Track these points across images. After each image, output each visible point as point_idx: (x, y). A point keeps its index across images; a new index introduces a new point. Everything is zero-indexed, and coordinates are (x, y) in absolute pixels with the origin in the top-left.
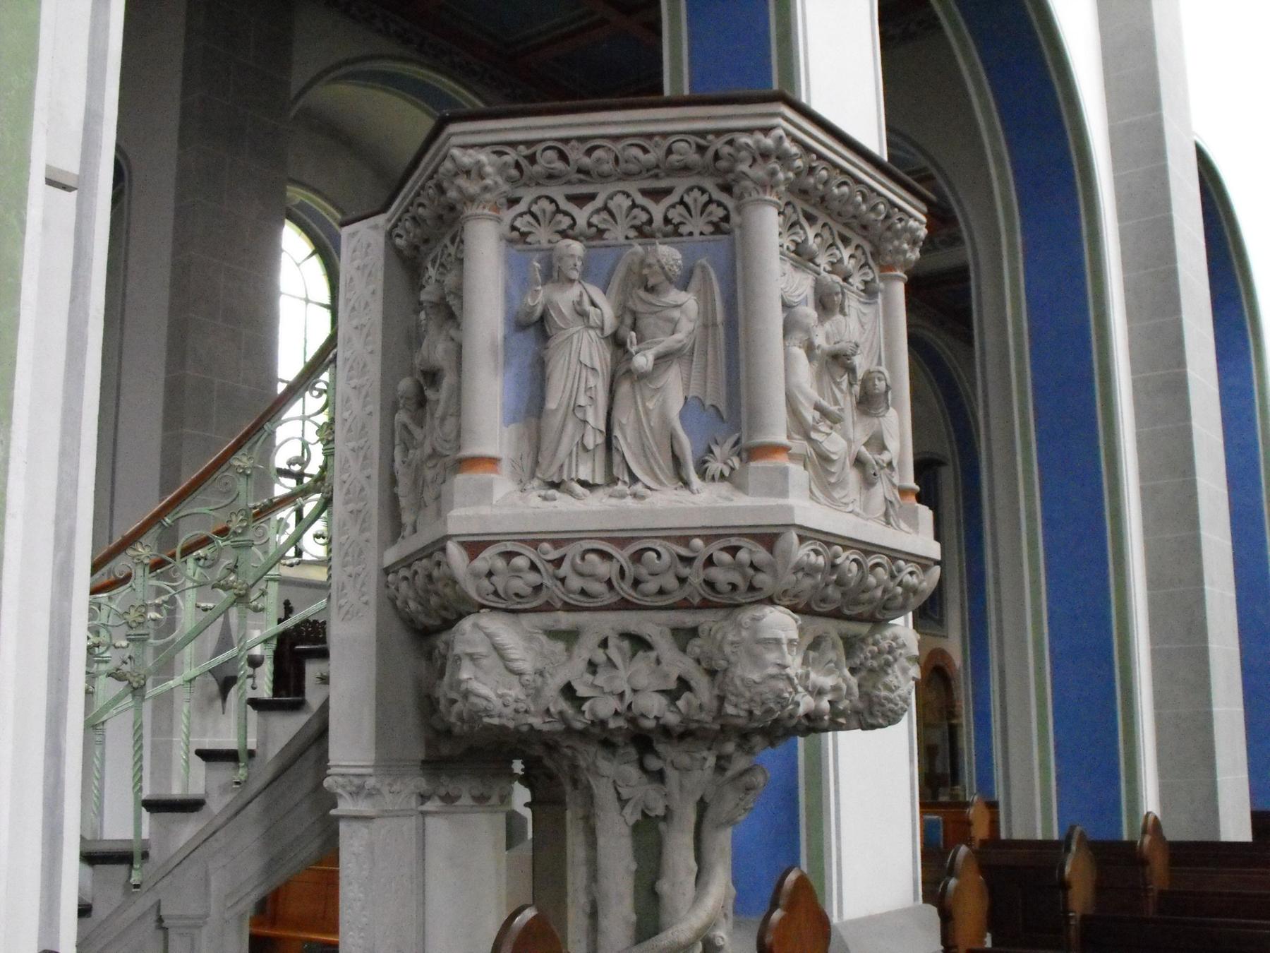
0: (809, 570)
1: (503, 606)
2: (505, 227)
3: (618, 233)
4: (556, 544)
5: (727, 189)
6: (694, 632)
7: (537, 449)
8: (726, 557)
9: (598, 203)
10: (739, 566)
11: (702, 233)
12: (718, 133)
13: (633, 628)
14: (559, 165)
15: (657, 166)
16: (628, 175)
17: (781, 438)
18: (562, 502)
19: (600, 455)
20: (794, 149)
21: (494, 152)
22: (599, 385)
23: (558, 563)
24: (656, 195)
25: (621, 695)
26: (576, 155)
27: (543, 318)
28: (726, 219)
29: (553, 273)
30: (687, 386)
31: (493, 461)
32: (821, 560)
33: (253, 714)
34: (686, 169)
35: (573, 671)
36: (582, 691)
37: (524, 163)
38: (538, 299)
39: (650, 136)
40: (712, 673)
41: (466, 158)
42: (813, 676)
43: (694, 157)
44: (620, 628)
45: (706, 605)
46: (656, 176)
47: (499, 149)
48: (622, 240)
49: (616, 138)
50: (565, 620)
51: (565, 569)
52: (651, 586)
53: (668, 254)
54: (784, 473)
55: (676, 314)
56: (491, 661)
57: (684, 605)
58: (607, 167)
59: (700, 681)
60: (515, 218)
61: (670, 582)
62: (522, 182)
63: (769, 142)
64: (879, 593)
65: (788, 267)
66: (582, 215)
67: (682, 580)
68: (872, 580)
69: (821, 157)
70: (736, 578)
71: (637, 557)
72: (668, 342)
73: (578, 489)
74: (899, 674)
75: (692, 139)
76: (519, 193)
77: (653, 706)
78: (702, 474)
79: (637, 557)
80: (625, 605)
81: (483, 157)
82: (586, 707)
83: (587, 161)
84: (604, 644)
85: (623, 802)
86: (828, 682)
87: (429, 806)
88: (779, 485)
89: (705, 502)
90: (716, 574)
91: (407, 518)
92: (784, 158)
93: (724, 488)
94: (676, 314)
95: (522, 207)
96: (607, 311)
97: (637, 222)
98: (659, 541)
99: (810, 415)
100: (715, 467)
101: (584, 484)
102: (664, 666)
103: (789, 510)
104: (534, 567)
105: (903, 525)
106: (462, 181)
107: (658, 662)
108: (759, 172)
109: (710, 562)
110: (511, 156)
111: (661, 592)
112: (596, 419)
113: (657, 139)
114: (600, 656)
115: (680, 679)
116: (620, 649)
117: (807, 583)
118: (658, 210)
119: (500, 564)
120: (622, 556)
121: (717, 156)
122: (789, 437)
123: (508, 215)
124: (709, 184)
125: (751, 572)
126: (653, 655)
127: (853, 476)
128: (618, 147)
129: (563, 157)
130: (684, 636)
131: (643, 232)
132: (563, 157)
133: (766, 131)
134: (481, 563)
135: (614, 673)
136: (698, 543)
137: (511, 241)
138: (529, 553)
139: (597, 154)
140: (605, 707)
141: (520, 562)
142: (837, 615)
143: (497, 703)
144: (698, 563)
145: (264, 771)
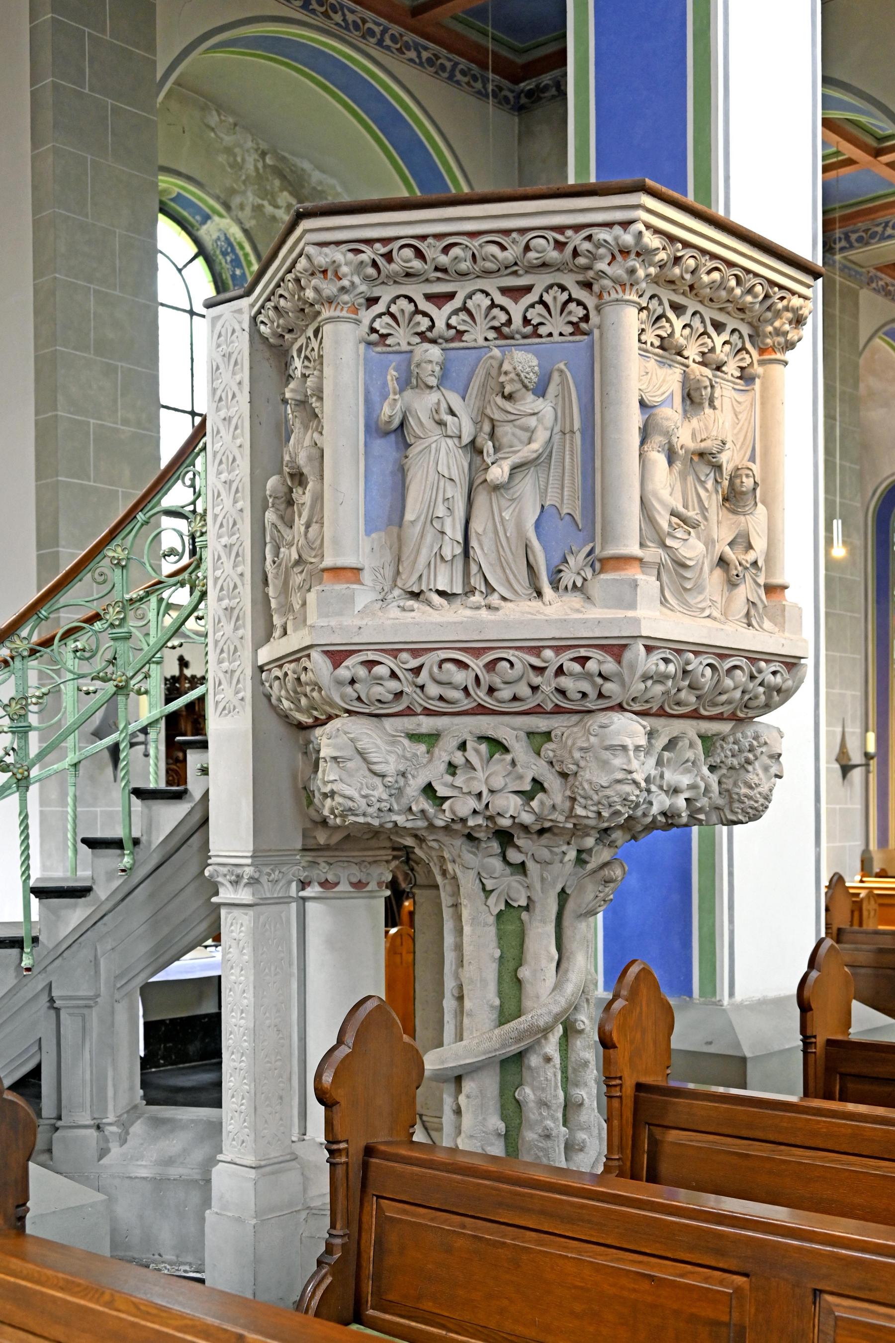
0: (661, 678)
1: (367, 711)
3: (478, 334)
4: (416, 653)
5: (587, 285)
6: (547, 736)
8: (577, 667)
9: (457, 303)
10: (588, 676)
11: (561, 334)
12: (577, 228)
13: (490, 733)
14: (417, 264)
15: (516, 264)
16: (487, 273)
17: (634, 549)
18: (420, 613)
19: (459, 564)
23: (417, 671)
25: (479, 795)
26: (432, 250)
29: (409, 380)
30: (544, 493)
35: (433, 772)
36: (442, 792)
37: (381, 261)
39: (507, 232)
40: (564, 775)
42: (668, 775)
43: (553, 255)
44: (479, 733)
45: (558, 711)
46: (515, 273)
47: (355, 246)
48: (481, 342)
49: (473, 235)
50: (426, 724)
52: (506, 693)
53: (524, 360)
54: (635, 585)
55: (532, 422)
57: (537, 711)
58: (463, 266)
59: (552, 781)
60: (374, 320)
61: (524, 690)
63: (628, 238)
64: (737, 694)
65: (652, 364)
67: (535, 689)
68: (728, 682)
69: (686, 245)
70: (586, 686)
73: (436, 599)
74: (760, 772)
77: (510, 806)
78: (555, 585)
79: (491, 666)
80: (481, 710)
81: (338, 255)
82: (446, 806)
83: (443, 260)
84: (463, 746)
85: (487, 893)
86: (685, 780)
88: (628, 597)
89: (556, 614)
90: (565, 682)
91: (277, 620)
92: (644, 253)
93: (575, 600)
94: (532, 422)
95: (380, 308)
97: (496, 324)
98: (511, 652)
99: (663, 521)
100: (568, 578)
101: (442, 594)
102: (519, 769)
103: (637, 621)
104: (393, 675)
105: (767, 624)
107: (513, 763)
108: (618, 270)
109: (560, 671)
110: (368, 254)
111: (515, 698)
113: (514, 235)
114: (458, 758)
115: (534, 780)
116: (477, 751)
117: (659, 689)
118: (517, 310)
119: (362, 672)
120: (477, 665)
121: (575, 253)
122: (642, 545)
123: (366, 316)
125: (599, 681)
126: (508, 757)
129: (419, 254)
130: (538, 739)
132: (419, 254)
133: (626, 224)
135: (472, 774)
136: (548, 654)
140: (465, 806)
141: (379, 670)
142: (695, 715)
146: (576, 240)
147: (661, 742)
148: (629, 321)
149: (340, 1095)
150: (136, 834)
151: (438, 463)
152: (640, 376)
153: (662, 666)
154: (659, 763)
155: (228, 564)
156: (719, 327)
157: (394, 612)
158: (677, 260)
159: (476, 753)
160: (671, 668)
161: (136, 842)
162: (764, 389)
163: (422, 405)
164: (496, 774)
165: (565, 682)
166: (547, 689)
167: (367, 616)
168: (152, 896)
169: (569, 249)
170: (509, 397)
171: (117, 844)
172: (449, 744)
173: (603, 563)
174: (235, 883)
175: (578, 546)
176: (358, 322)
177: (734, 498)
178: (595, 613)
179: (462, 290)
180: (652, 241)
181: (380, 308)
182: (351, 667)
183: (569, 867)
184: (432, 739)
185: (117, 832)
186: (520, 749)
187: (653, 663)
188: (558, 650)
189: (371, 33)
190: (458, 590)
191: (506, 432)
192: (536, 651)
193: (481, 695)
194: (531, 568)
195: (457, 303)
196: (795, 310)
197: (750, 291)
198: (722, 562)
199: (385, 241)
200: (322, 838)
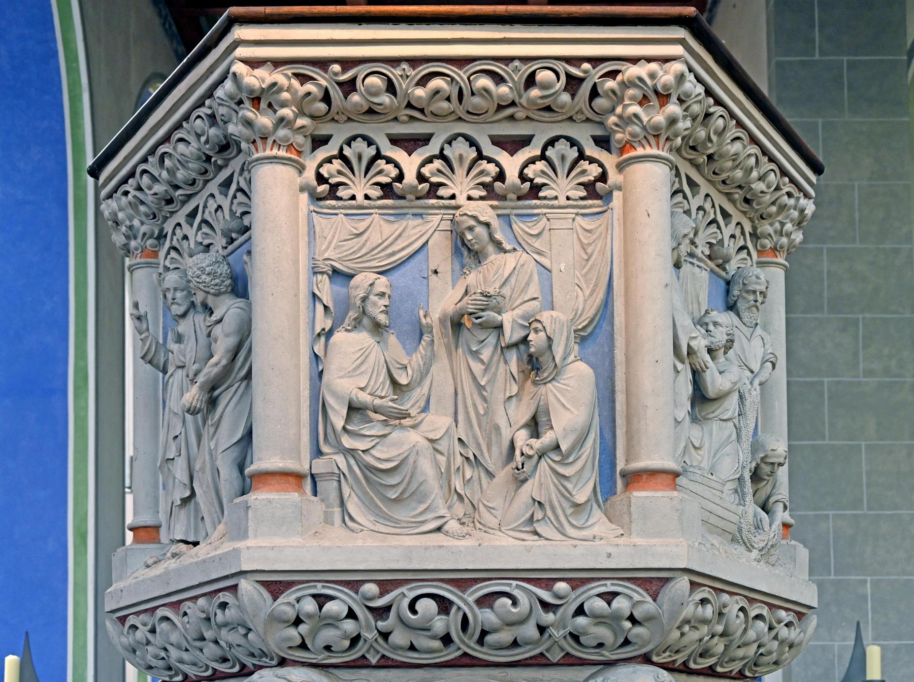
2: (310, 175)
8: (600, 604)
9: (433, 148)
15: (513, 104)
21: (296, 75)
28: (603, 178)
41: (255, 79)
46: (512, 118)
47: (303, 69)
62: (329, 117)
75: (561, 67)
76: (324, 130)
95: (331, 150)
119: (310, 606)
121: (594, 93)
125: (628, 624)
134: (285, 605)
136: (561, 586)
137: (317, 198)
139: (437, 83)
166: (558, 634)
169: (585, 90)
181: (331, 150)
195: (433, 148)
199: (347, 63)
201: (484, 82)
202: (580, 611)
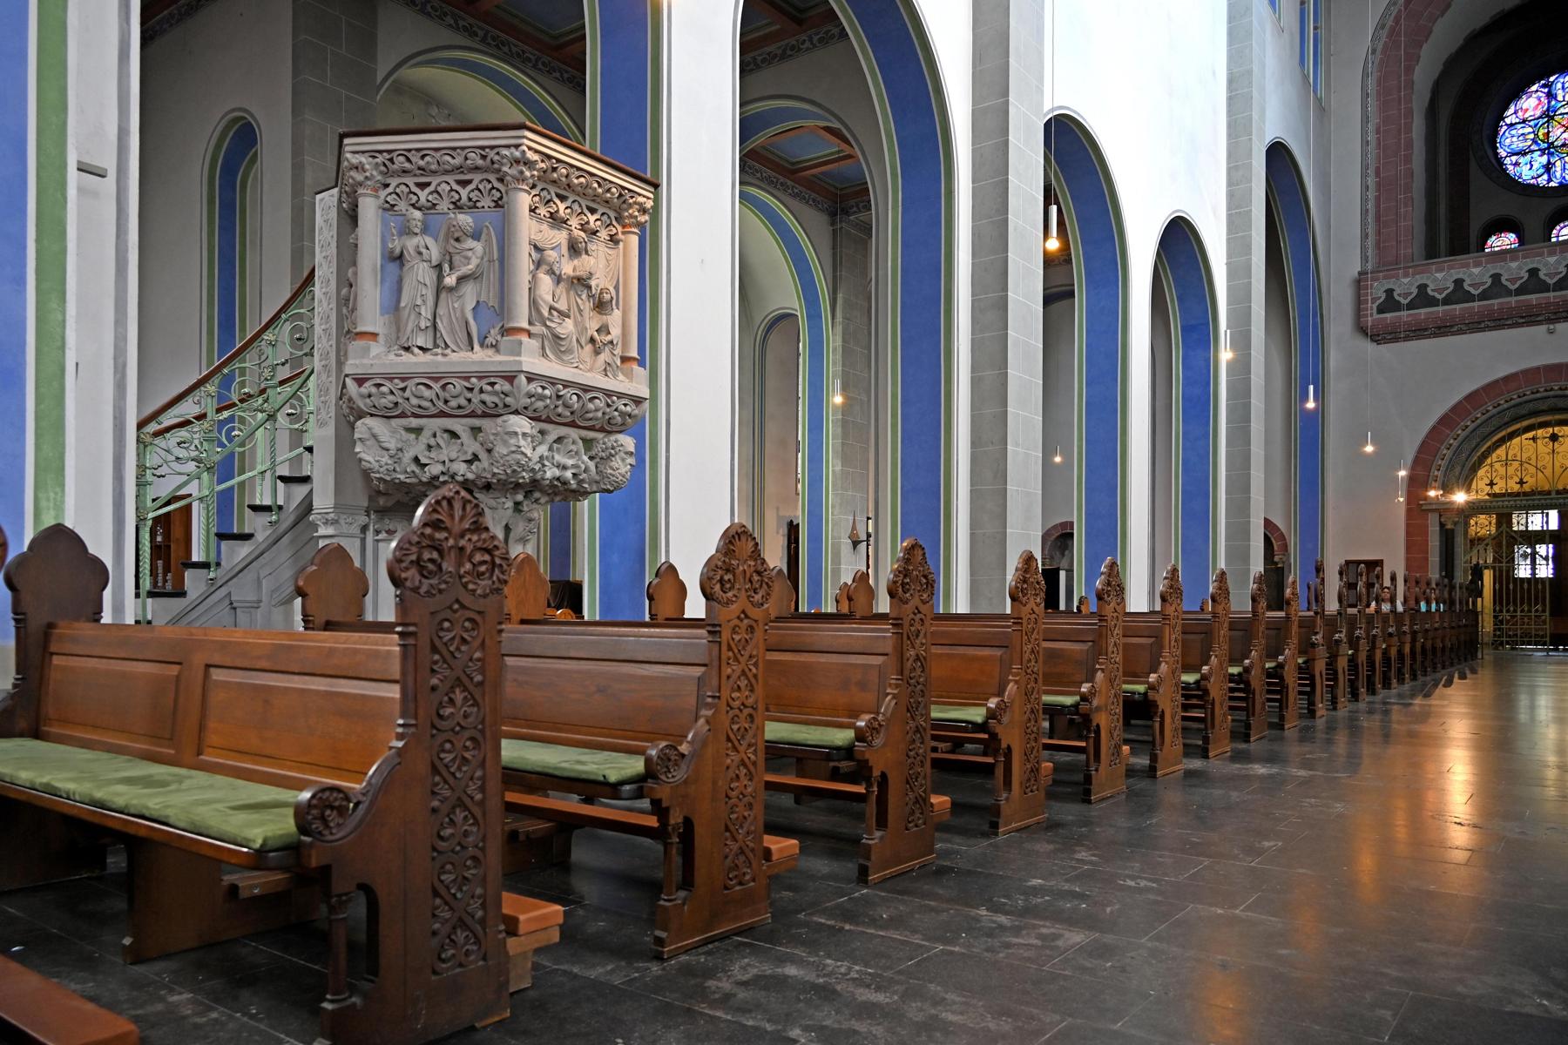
0: (542, 398)
3: (444, 206)
4: (403, 380)
5: (501, 180)
6: (479, 429)
7: (398, 330)
8: (489, 388)
9: (432, 188)
10: (496, 393)
12: (492, 148)
13: (449, 427)
14: (407, 165)
16: (447, 172)
17: (525, 325)
18: (407, 357)
20: (536, 157)
22: (430, 295)
23: (404, 389)
24: (464, 183)
26: (415, 158)
27: (401, 255)
29: (406, 231)
30: (479, 295)
31: (374, 335)
32: (547, 392)
33: (280, 485)
34: (477, 169)
35: (418, 449)
36: (424, 460)
38: (396, 245)
39: (454, 149)
40: (489, 451)
42: (557, 457)
43: (480, 162)
45: (485, 415)
47: (373, 154)
50: (414, 422)
51: (408, 393)
52: (453, 403)
53: (465, 220)
54: (520, 343)
55: (470, 254)
56: (371, 442)
57: (472, 415)
58: (434, 167)
59: (483, 455)
63: (517, 154)
64: (600, 414)
65: (545, 227)
66: (423, 195)
67: (469, 400)
68: (591, 406)
69: (558, 161)
70: (496, 400)
71: (444, 387)
72: (465, 270)
73: (416, 350)
76: (388, 181)
78: (482, 345)
79: (444, 387)
80: (442, 414)
81: (363, 159)
83: (422, 163)
84: (435, 436)
86: (570, 462)
87: (380, 537)
88: (517, 350)
89: (481, 357)
90: (484, 397)
92: (529, 164)
93: (490, 352)
94: (470, 254)
95: (390, 189)
96: (435, 254)
100: (490, 340)
101: (420, 348)
103: (520, 363)
105: (621, 377)
106: (353, 173)
108: (513, 172)
109: (481, 391)
110: (380, 159)
112: (426, 312)
114: (432, 442)
117: (540, 404)
118: (464, 193)
119: (374, 390)
120: (436, 386)
122: (530, 323)
123: (383, 193)
124: (492, 177)
127: (589, 348)
128: (437, 155)
129: (408, 160)
130: (476, 431)
131: (457, 206)
132: (408, 160)
133: (517, 146)
136: (474, 380)
138: (387, 383)
140: (436, 469)
141: (383, 389)
142: (573, 425)
143: (376, 466)
144: (476, 390)
145: (288, 518)
146: (492, 154)
147: (551, 437)
148: (524, 200)
149: (308, 590)
150: (280, 502)
151: (421, 273)
152: (528, 228)
153: (540, 390)
154: (550, 449)
155: (324, 340)
156: (593, 211)
157: (392, 356)
158: (554, 169)
159: (442, 439)
160: (547, 392)
161: (280, 508)
162: (625, 248)
163: (411, 243)
164: (449, 451)
165: (484, 397)
167: (376, 357)
168: (292, 542)
170: (457, 240)
171: (267, 509)
172: (427, 433)
173: (506, 331)
174: (326, 523)
175: (496, 323)
176: (377, 197)
177: (601, 306)
178: (499, 358)
179: (435, 181)
180: (531, 155)
181: (390, 189)
182: (368, 387)
183: (510, 512)
184: (418, 431)
185: (267, 502)
186: (465, 436)
187: (534, 387)
188: (480, 378)
189: (529, 60)
190: (430, 346)
191: (456, 258)
192: (467, 379)
193: (441, 404)
194: (469, 335)
195: (432, 188)
196: (640, 204)
197: (609, 190)
198: (592, 340)
199: (389, 152)
200: (381, 501)
201: (448, 158)
202: (481, 391)
